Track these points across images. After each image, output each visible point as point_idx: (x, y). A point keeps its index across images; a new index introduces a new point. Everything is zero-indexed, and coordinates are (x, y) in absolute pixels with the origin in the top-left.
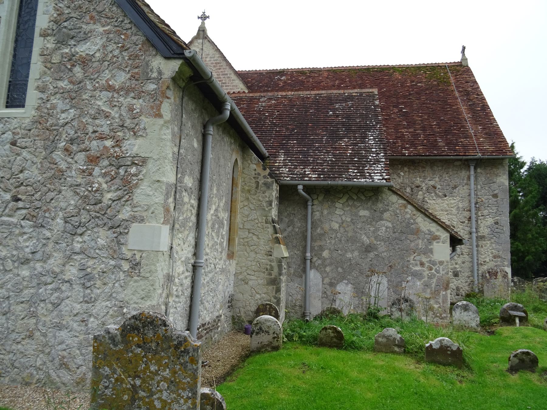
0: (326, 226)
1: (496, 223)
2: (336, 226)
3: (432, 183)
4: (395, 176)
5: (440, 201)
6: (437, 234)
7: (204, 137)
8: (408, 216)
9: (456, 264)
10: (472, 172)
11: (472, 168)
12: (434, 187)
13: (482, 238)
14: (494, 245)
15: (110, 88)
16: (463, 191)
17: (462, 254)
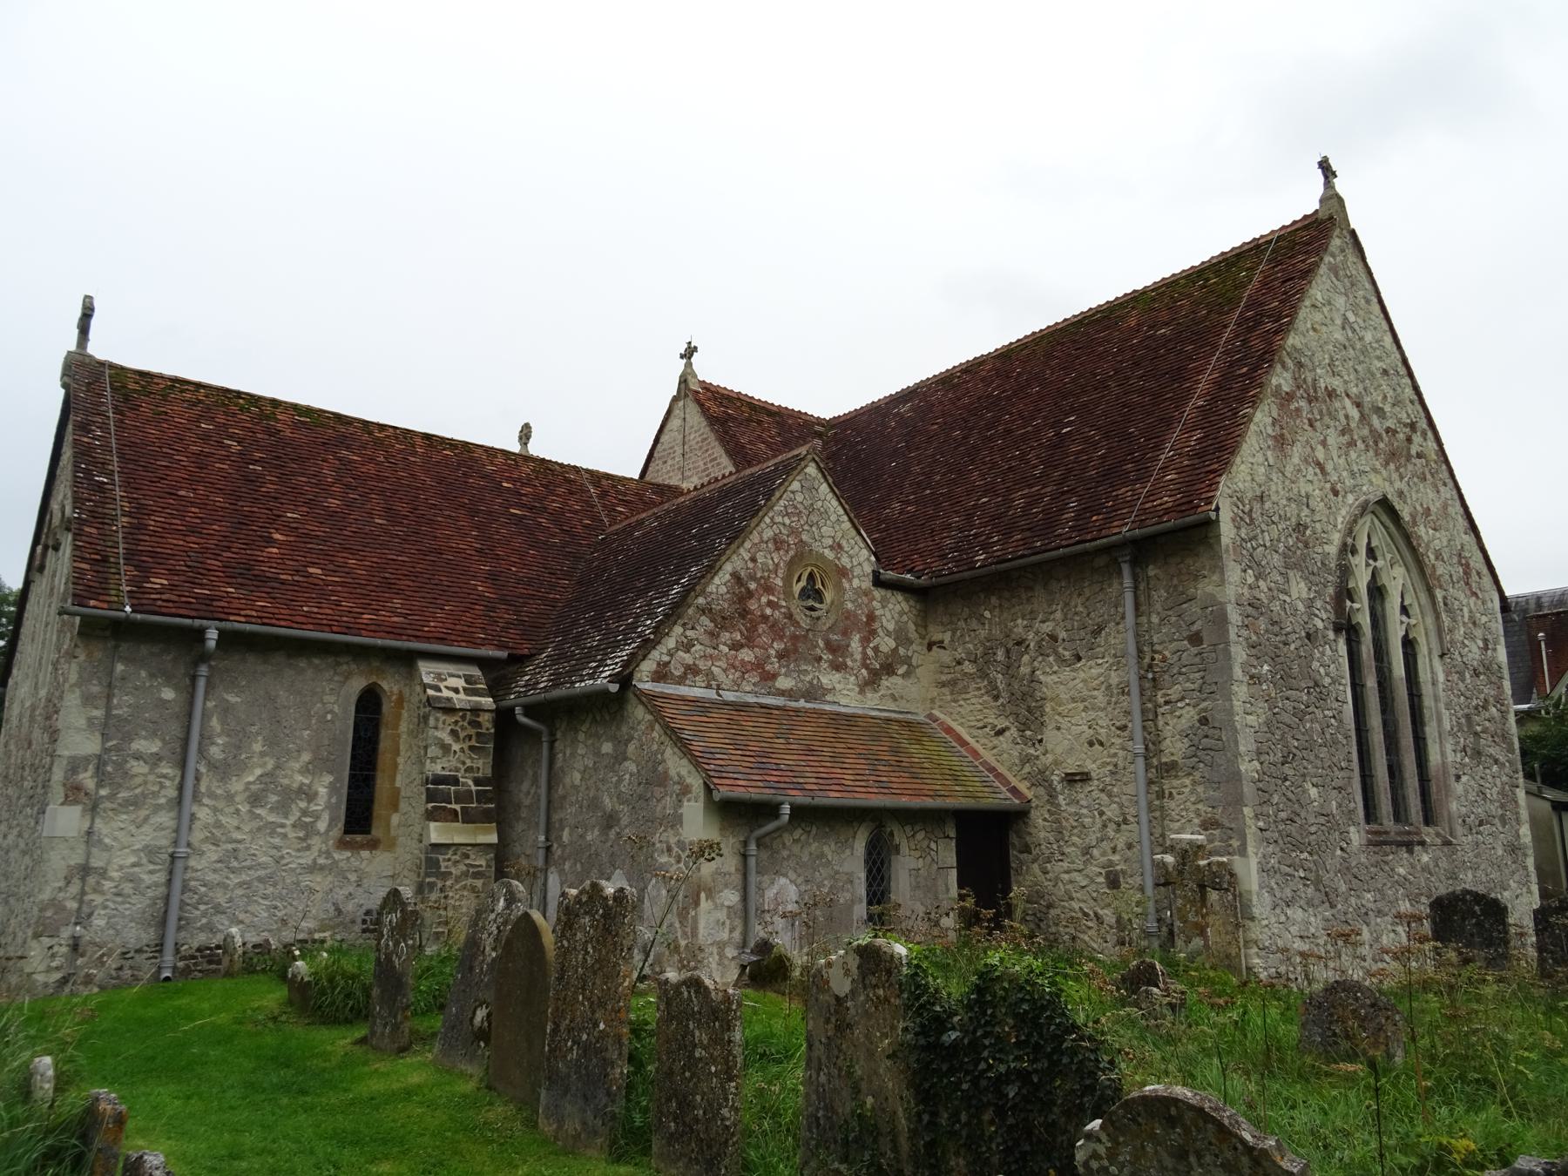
0: (567, 780)
1: (1204, 721)
2: (577, 776)
3: (1047, 627)
4: (974, 624)
5: (1067, 673)
6: (689, 781)
7: (194, 679)
8: (655, 747)
9: (1114, 850)
10: (1128, 581)
11: (1126, 569)
12: (1054, 638)
13: (1170, 769)
14: (1200, 789)
16: (1120, 637)
17: (1125, 821)
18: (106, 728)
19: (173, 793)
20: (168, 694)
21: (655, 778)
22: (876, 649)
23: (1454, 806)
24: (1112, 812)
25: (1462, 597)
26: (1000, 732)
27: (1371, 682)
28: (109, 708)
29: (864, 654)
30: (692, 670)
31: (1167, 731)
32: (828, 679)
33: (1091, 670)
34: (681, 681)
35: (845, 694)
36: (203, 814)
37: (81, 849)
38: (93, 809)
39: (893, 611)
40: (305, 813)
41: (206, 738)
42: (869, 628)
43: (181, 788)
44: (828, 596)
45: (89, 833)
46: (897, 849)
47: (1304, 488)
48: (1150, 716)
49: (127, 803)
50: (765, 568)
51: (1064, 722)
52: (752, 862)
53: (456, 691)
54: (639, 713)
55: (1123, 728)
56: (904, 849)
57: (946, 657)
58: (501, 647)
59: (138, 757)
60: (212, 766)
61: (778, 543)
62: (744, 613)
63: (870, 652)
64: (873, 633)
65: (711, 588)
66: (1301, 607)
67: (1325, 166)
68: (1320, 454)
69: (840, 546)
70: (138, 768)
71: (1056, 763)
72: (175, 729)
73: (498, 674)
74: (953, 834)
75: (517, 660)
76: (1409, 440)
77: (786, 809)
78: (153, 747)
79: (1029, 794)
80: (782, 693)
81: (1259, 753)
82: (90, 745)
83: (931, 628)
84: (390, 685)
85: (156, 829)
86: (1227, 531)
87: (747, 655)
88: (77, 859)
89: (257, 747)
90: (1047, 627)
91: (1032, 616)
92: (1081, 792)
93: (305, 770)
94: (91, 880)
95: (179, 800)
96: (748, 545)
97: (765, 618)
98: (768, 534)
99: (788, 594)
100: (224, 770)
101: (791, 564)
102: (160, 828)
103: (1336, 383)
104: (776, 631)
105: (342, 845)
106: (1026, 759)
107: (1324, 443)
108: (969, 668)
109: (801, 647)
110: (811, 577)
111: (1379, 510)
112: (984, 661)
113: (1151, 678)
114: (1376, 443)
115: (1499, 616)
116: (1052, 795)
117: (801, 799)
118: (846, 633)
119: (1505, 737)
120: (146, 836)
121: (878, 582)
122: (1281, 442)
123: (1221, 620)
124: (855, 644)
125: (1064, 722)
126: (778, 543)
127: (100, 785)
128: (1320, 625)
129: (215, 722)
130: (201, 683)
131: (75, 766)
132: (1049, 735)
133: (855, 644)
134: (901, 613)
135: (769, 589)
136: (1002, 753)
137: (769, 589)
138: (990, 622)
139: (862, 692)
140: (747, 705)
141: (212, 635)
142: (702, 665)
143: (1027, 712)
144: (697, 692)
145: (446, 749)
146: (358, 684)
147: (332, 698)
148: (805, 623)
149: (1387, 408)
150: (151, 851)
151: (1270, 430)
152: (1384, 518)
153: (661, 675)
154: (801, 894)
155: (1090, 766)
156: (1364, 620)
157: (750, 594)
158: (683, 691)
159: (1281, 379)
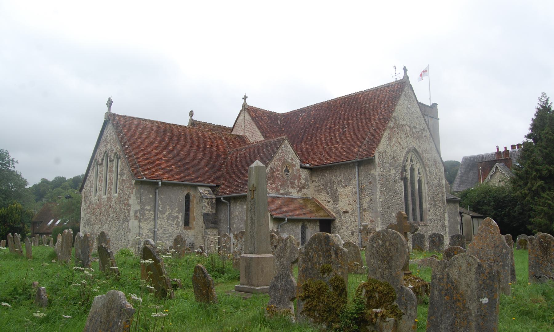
0: (235, 214)
1: (371, 200)
2: (237, 213)
3: (340, 179)
4: (323, 177)
5: (344, 189)
7: (156, 193)
10: (357, 170)
11: (356, 167)
12: (341, 181)
13: (364, 210)
15: (126, 187)
16: (355, 181)
18: (141, 203)
19: (153, 217)
20: (151, 196)
22: (301, 183)
23: (428, 217)
24: (353, 219)
25: (434, 169)
26: (329, 202)
27: (409, 190)
28: (141, 199)
31: (364, 202)
32: (291, 190)
33: (349, 189)
35: (295, 194)
36: (159, 222)
38: (140, 221)
39: (304, 174)
40: (177, 221)
43: (155, 216)
44: (290, 171)
47: (395, 148)
48: (361, 199)
51: (343, 200)
55: (355, 201)
57: (316, 184)
58: (214, 183)
60: (160, 211)
61: (280, 159)
62: (273, 176)
64: (300, 179)
68: (399, 140)
70: (147, 212)
71: (341, 209)
72: (153, 204)
75: (218, 186)
76: (422, 133)
77: (286, 219)
79: (335, 216)
80: (281, 194)
82: (138, 208)
84: (192, 193)
85: (150, 226)
86: (377, 160)
87: (274, 186)
88: (138, 232)
89: (168, 207)
90: (340, 179)
91: (336, 176)
92: (346, 215)
93: (177, 212)
97: (277, 177)
98: (278, 158)
99: (282, 171)
100: (162, 212)
101: (282, 164)
102: (151, 225)
103: (404, 123)
105: (185, 228)
106: (335, 208)
107: (400, 137)
108: (322, 187)
112: (325, 185)
113: (361, 191)
116: (340, 216)
117: (289, 217)
118: (294, 180)
119: (443, 201)
122: (390, 139)
123: (375, 179)
124: (296, 182)
125: (343, 200)
130: (157, 194)
131: (136, 212)
132: (340, 202)
133: (296, 182)
135: (278, 170)
136: (329, 206)
137: (278, 170)
138: (327, 176)
141: (160, 183)
143: (335, 197)
145: (206, 207)
146: (185, 193)
147: (180, 195)
148: (285, 177)
149: (417, 126)
150: (150, 230)
155: (348, 209)
156: (409, 177)
157: (274, 172)
159: (391, 124)
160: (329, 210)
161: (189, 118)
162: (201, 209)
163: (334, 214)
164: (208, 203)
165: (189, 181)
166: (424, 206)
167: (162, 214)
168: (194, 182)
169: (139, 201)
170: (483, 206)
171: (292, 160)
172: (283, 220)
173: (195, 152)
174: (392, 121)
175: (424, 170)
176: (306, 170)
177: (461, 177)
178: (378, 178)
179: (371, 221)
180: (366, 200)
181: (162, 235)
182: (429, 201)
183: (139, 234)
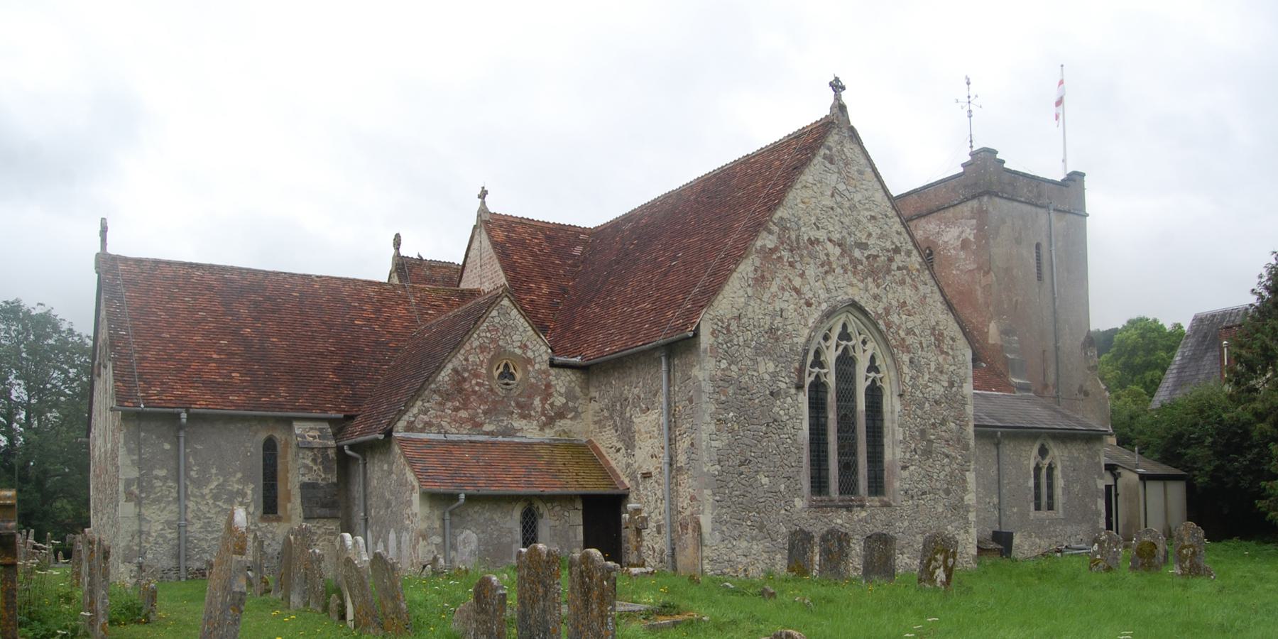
1: (692, 444)
3: (636, 391)
5: (644, 417)
10: (664, 367)
18: (140, 464)
20: (167, 446)
21: (402, 483)
22: (552, 405)
23: (897, 484)
25: (930, 355)
27: (832, 416)
29: (543, 408)
30: (429, 424)
33: (653, 416)
34: (422, 430)
35: (530, 432)
36: (191, 505)
37: (137, 522)
38: (139, 503)
39: (562, 382)
41: (188, 468)
42: (547, 392)
43: (178, 492)
44: (518, 376)
45: (139, 515)
46: (542, 516)
47: (778, 305)
49: (154, 501)
50: (474, 363)
51: (642, 444)
52: (447, 522)
53: (314, 437)
54: (397, 449)
56: (546, 514)
58: (339, 412)
59: (157, 478)
60: (193, 481)
61: (482, 348)
62: (461, 391)
63: (547, 406)
64: (550, 395)
65: (440, 378)
66: (767, 377)
67: (837, 86)
68: (797, 282)
69: (526, 346)
70: (158, 483)
71: (640, 467)
73: (339, 426)
74: (580, 507)
75: (349, 418)
76: (891, 260)
77: (462, 496)
78: (162, 473)
80: (487, 433)
81: (719, 461)
82: (135, 473)
83: (592, 389)
84: (280, 435)
85: (171, 512)
86: (705, 339)
87: (463, 414)
88: (136, 527)
89: (214, 471)
90: (636, 391)
93: (239, 482)
94: (144, 537)
95: (178, 499)
96: (462, 351)
97: (475, 392)
98: (476, 344)
99: (490, 377)
100: (199, 483)
101: (491, 362)
102: (171, 512)
103: (822, 235)
104: (481, 397)
106: (628, 465)
107: (802, 275)
109: (499, 407)
110: (506, 366)
111: (851, 309)
114: (855, 267)
115: (970, 365)
117: (471, 490)
118: (531, 397)
119: (960, 441)
120: (166, 516)
121: (552, 364)
122: (760, 280)
123: (699, 390)
124: (537, 402)
125: (642, 444)
126: (482, 348)
127: (141, 492)
128: (783, 386)
129: (191, 459)
131: (128, 483)
132: (637, 452)
133: (537, 402)
134: (570, 382)
135: (477, 376)
137: (477, 376)
139: (542, 429)
140: (462, 442)
142: (434, 421)
143: (628, 439)
144: (432, 436)
145: (310, 469)
146: (262, 436)
147: (251, 443)
148: (501, 392)
150: (168, 523)
151: (751, 275)
152: (857, 314)
153: (410, 427)
154: (479, 540)
156: (831, 381)
157: (464, 380)
158: (423, 436)
159: (767, 240)
160: (618, 471)
161: (392, 251)
162: (298, 473)
163: (626, 481)
164: (314, 460)
165: (267, 409)
166: (888, 455)
167: (199, 487)
168: (281, 409)
169: (136, 457)
170: (1188, 446)
171: (524, 347)
172: (453, 497)
173: (313, 338)
174: (770, 232)
175: (889, 360)
176: (569, 372)
177: (1181, 369)
178: (708, 387)
179: (693, 498)
180: (683, 445)
181: (202, 536)
182: (904, 441)
183: (141, 532)
